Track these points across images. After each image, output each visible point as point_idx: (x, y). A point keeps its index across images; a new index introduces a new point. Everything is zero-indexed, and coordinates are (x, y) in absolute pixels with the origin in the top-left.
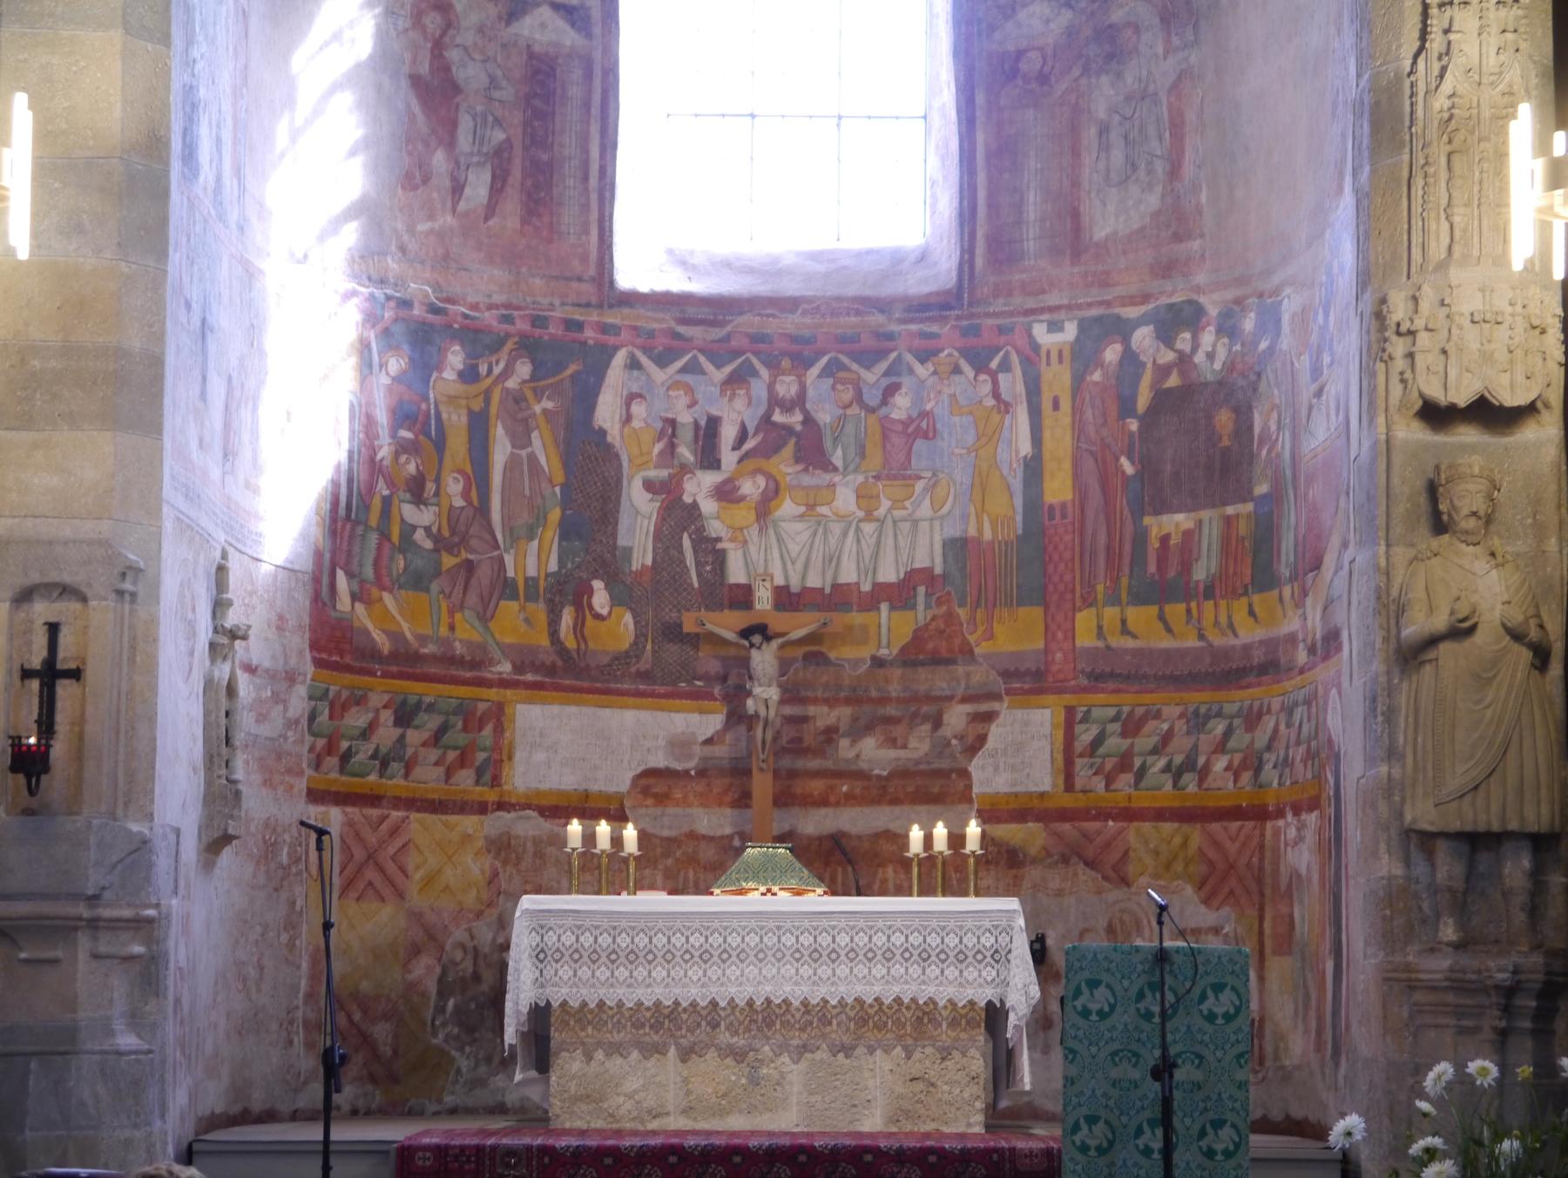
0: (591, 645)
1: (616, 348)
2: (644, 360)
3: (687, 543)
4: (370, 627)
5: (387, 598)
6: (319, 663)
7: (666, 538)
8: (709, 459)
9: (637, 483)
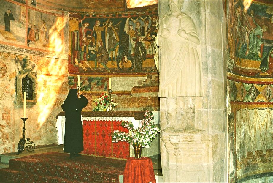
0: (125, 67)
1: (127, 18)
2: (132, 19)
3: (140, 49)
4: (83, 67)
5: (86, 62)
6: (70, 73)
7: (136, 49)
8: (143, 34)
9: (132, 40)
